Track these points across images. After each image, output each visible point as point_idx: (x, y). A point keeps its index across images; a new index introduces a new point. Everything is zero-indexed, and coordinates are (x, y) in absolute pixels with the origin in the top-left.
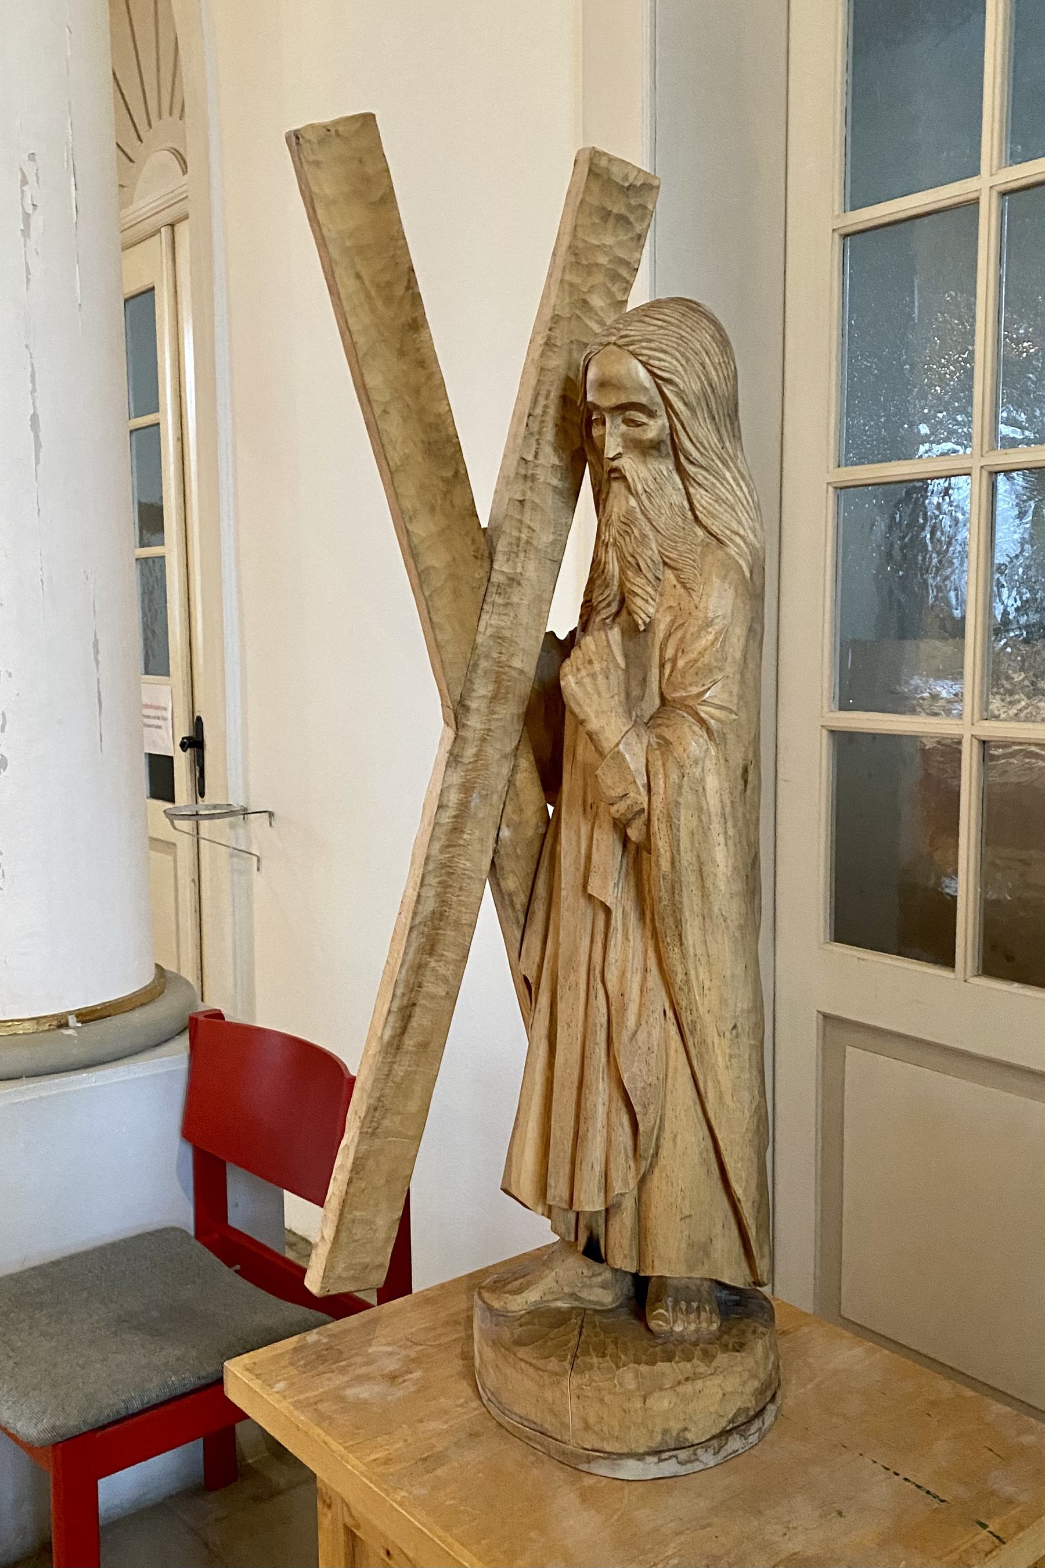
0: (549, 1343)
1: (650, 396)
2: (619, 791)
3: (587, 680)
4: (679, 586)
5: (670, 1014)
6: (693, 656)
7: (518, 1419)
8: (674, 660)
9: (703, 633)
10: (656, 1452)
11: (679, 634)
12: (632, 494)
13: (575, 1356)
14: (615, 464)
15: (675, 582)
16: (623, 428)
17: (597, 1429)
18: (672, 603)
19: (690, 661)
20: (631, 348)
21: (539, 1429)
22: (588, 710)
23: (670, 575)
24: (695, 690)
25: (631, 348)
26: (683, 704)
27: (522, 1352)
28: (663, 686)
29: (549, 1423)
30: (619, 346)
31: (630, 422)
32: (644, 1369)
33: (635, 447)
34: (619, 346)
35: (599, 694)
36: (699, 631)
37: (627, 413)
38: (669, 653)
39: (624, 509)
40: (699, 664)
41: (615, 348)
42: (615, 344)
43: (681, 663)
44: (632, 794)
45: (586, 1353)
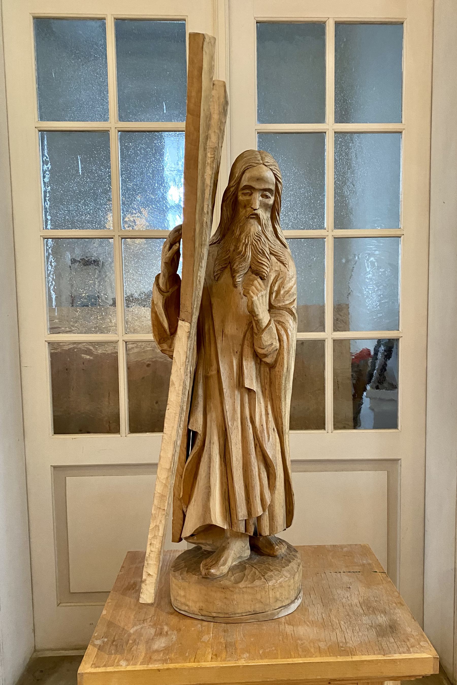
0: (249, 577)
1: (273, 188)
2: (269, 343)
3: (260, 298)
4: (278, 262)
5: (275, 429)
6: (286, 289)
7: (240, 615)
8: (278, 292)
9: (291, 281)
10: (296, 598)
11: (282, 280)
12: (260, 225)
13: (263, 576)
14: (256, 212)
15: (276, 261)
16: (261, 198)
17: (280, 599)
18: (277, 269)
19: (286, 291)
20: (270, 167)
21: (253, 613)
22: (259, 310)
23: (273, 258)
24: (287, 302)
25: (270, 167)
26: (280, 308)
27: (242, 585)
28: (272, 301)
29: (258, 607)
30: (266, 165)
31: (262, 196)
32: (287, 568)
33: (264, 206)
34: (266, 165)
35: (263, 303)
36: (289, 280)
37: (265, 192)
38: (276, 288)
39: (257, 230)
40: (291, 293)
41: (264, 166)
42: (264, 164)
43: (282, 292)
44: (274, 343)
45: (266, 573)
